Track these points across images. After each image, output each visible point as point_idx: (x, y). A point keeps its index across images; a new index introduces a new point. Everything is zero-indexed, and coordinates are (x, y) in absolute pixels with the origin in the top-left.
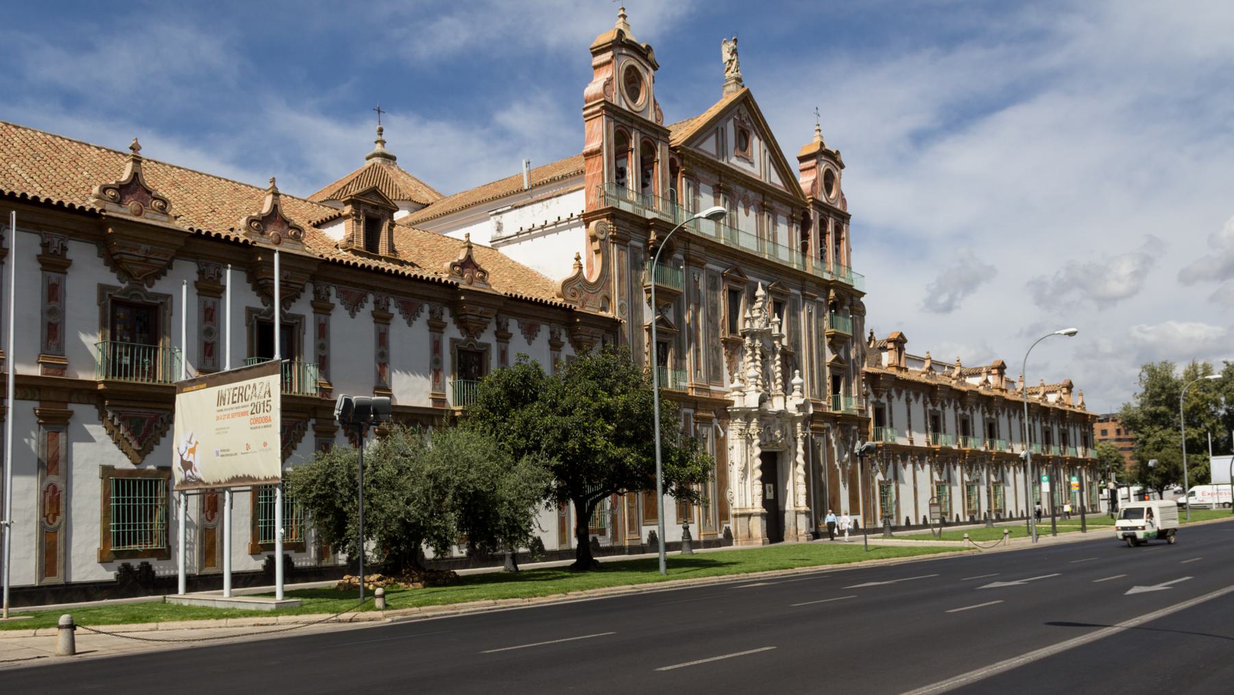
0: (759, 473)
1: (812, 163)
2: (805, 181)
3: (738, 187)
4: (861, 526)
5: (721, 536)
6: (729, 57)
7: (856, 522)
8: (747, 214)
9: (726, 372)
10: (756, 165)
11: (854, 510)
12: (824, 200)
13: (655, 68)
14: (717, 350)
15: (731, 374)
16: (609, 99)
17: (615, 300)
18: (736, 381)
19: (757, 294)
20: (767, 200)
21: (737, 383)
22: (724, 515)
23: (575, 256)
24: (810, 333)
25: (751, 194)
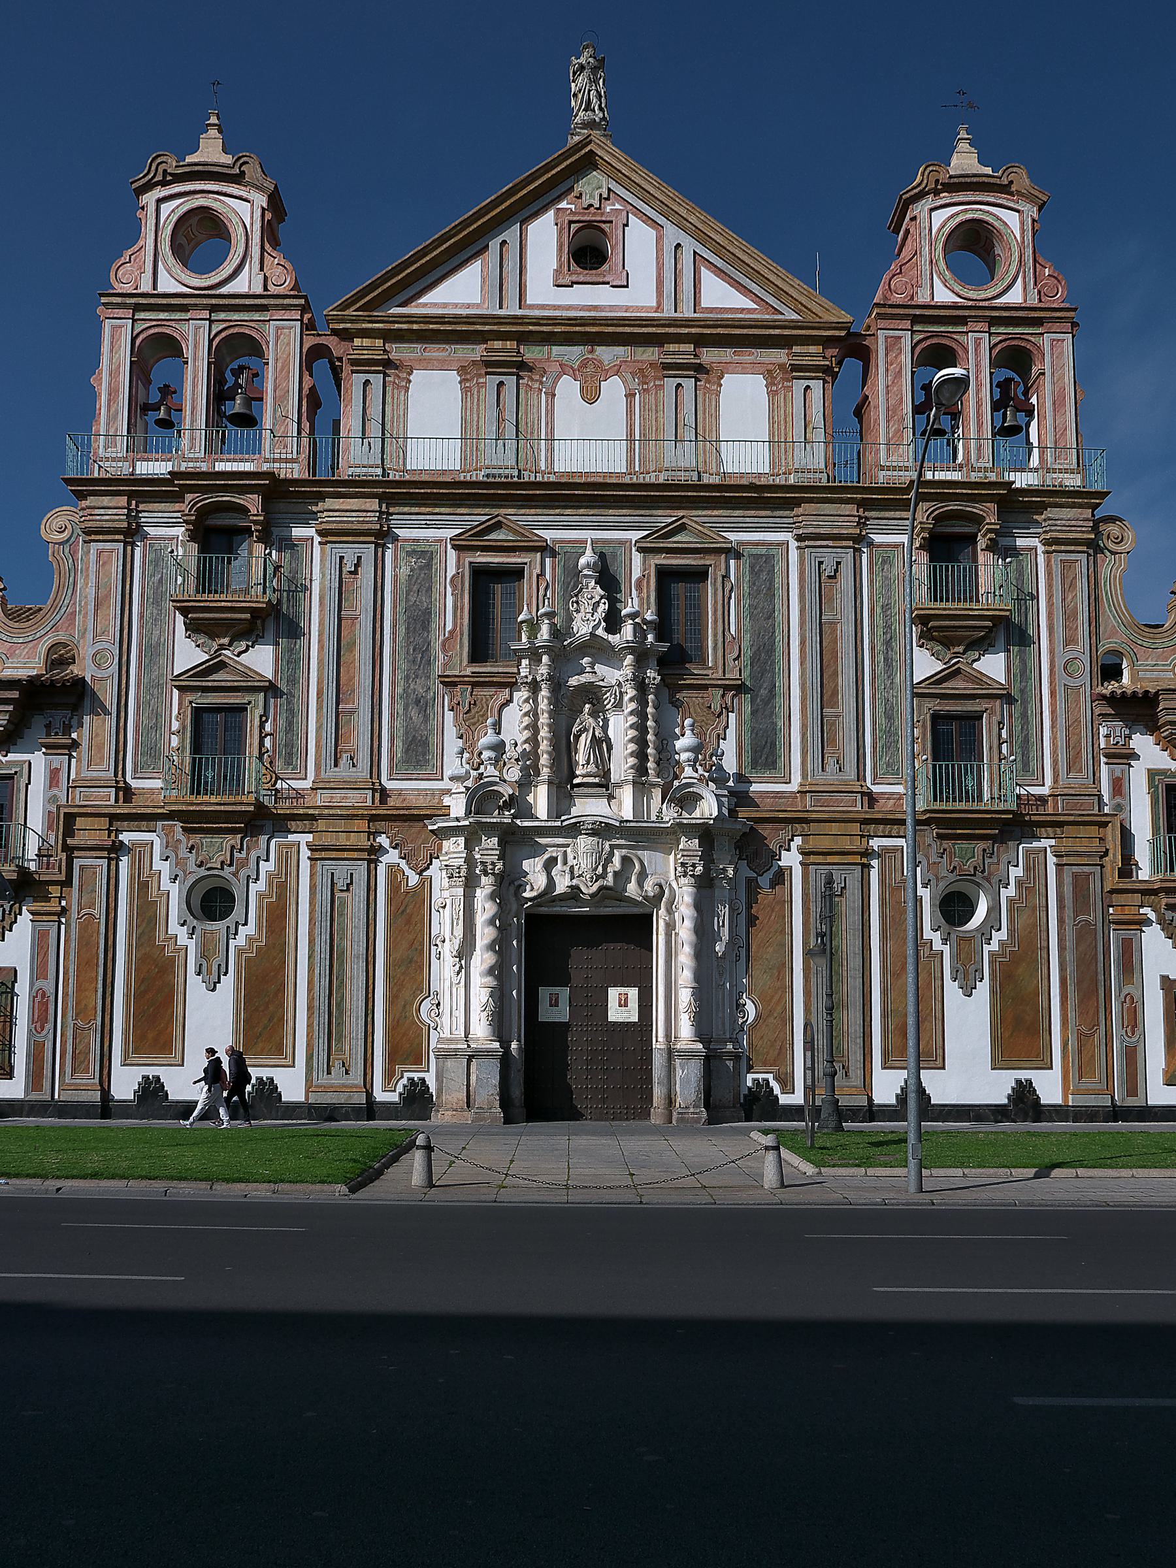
3: (556, 349)
14: (423, 705)
25: (606, 354)
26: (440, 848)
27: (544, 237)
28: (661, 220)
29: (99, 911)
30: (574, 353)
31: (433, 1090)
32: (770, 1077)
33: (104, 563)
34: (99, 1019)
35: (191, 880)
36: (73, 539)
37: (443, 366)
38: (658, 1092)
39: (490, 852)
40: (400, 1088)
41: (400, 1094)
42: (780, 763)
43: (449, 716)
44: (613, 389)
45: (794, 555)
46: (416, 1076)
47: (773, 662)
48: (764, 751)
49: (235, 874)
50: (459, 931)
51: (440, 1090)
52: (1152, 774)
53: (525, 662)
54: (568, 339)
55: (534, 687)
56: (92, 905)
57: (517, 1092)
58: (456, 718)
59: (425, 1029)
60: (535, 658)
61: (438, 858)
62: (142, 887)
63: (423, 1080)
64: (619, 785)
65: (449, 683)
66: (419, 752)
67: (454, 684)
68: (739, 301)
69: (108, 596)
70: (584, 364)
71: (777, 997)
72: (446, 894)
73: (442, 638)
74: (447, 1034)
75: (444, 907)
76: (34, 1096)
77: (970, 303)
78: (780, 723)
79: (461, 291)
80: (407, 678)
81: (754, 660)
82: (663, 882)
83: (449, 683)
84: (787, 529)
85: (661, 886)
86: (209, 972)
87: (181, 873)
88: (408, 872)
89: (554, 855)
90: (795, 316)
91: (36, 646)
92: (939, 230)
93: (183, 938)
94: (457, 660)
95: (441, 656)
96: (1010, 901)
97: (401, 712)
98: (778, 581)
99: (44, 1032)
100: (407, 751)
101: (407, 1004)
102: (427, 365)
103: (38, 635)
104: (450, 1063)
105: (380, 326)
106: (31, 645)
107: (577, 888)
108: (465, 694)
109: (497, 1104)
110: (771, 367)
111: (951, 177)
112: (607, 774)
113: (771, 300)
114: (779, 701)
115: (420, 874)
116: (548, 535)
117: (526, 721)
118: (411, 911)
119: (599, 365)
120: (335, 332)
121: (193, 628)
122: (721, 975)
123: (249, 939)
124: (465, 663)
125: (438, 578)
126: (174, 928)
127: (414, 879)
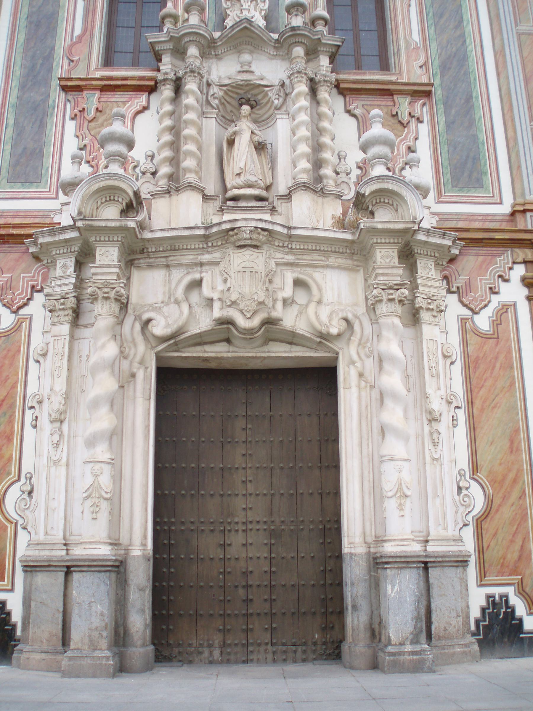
31: (17, 617)
32: (510, 591)
38: (356, 621)
42: (487, 180)
43: (71, 126)
47: (467, 74)
48: (464, 169)
50: (60, 386)
53: (166, 59)
55: (178, 87)
57: (139, 621)
58: (79, 128)
59: (10, 528)
60: (180, 52)
61: (41, 290)
64: (288, 197)
65: (70, 88)
67: (79, 89)
71: (511, 476)
72: (48, 338)
73: (68, 42)
74: (41, 537)
75: (44, 355)
78: (482, 136)
80: (22, 87)
81: (444, 68)
82: (350, 316)
83: (70, 88)
85: (346, 320)
89: (197, 276)
94: (82, 65)
95: (66, 62)
97: (11, 122)
104: (40, 579)
107: (230, 322)
108: (92, 100)
109: (104, 643)
112: (268, 188)
114: (479, 113)
115: (15, 312)
117: (168, 122)
122: (435, 444)
124: (93, 66)
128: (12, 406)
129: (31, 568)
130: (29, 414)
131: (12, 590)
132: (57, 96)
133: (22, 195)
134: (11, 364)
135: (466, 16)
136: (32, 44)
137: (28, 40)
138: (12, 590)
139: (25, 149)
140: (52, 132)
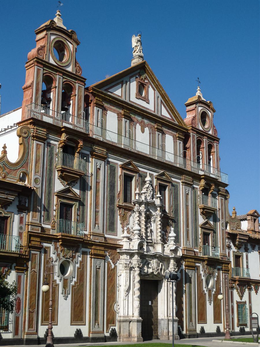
0: (138, 293)
1: (193, 107)
2: (188, 118)
4: (222, 330)
5: (107, 335)
6: (136, 44)
7: (218, 328)
8: (143, 131)
9: (119, 226)
10: (151, 102)
11: (217, 319)
12: (201, 128)
13: (78, 44)
15: (123, 227)
16: (41, 57)
17: (33, 176)
18: (125, 232)
19: (146, 179)
20: (160, 125)
21: (126, 234)
22: (111, 321)
23: (3, 146)
24: (187, 206)
25: (146, 121)
26: (119, 257)
27: (134, 86)
28: (155, 89)
29: (37, 270)
30: (140, 119)
33: (38, 149)
34: (36, 309)
35: (61, 261)
36: (28, 137)
37: (114, 111)
39: (128, 260)
40: (110, 332)
41: (110, 334)
43: (119, 217)
44: (147, 130)
45: (181, 186)
46: (113, 327)
49: (72, 260)
51: (120, 332)
52: (234, 252)
54: (139, 115)
56: (35, 268)
61: (119, 260)
62: (48, 261)
63: (115, 329)
65: (120, 207)
66: (112, 227)
68: (168, 116)
69: (39, 160)
70: (141, 122)
76: (16, 337)
77: (205, 131)
78: (179, 230)
79: (118, 92)
80: (110, 204)
83: (120, 207)
84: (180, 179)
86: (65, 293)
87: (58, 259)
88: (112, 264)
90: (176, 123)
91: (17, 171)
92: (200, 112)
93: (58, 282)
96: (216, 281)
98: (178, 192)
99: (19, 313)
100: (110, 226)
101: (111, 307)
102: (111, 110)
103: (18, 168)
105: (103, 96)
106: (15, 171)
108: (122, 211)
110: (174, 135)
111: (202, 100)
113: (174, 118)
116: (140, 169)
118: (112, 275)
119: (144, 123)
120: (92, 93)
121: (61, 177)
123: (75, 283)
125: (116, 175)
126: (56, 278)
127: (113, 266)
128: (115, 286)
129: (120, 321)
130: (117, 288)
131: (116, 326)
132: (116, 209)
133: (111, 234)
134: (114, 276)
135: (178, 199)
136: (111, 192)
137: (110, 190)
138: (116, 326)
139: (111, 222)
140: (115, 218)
